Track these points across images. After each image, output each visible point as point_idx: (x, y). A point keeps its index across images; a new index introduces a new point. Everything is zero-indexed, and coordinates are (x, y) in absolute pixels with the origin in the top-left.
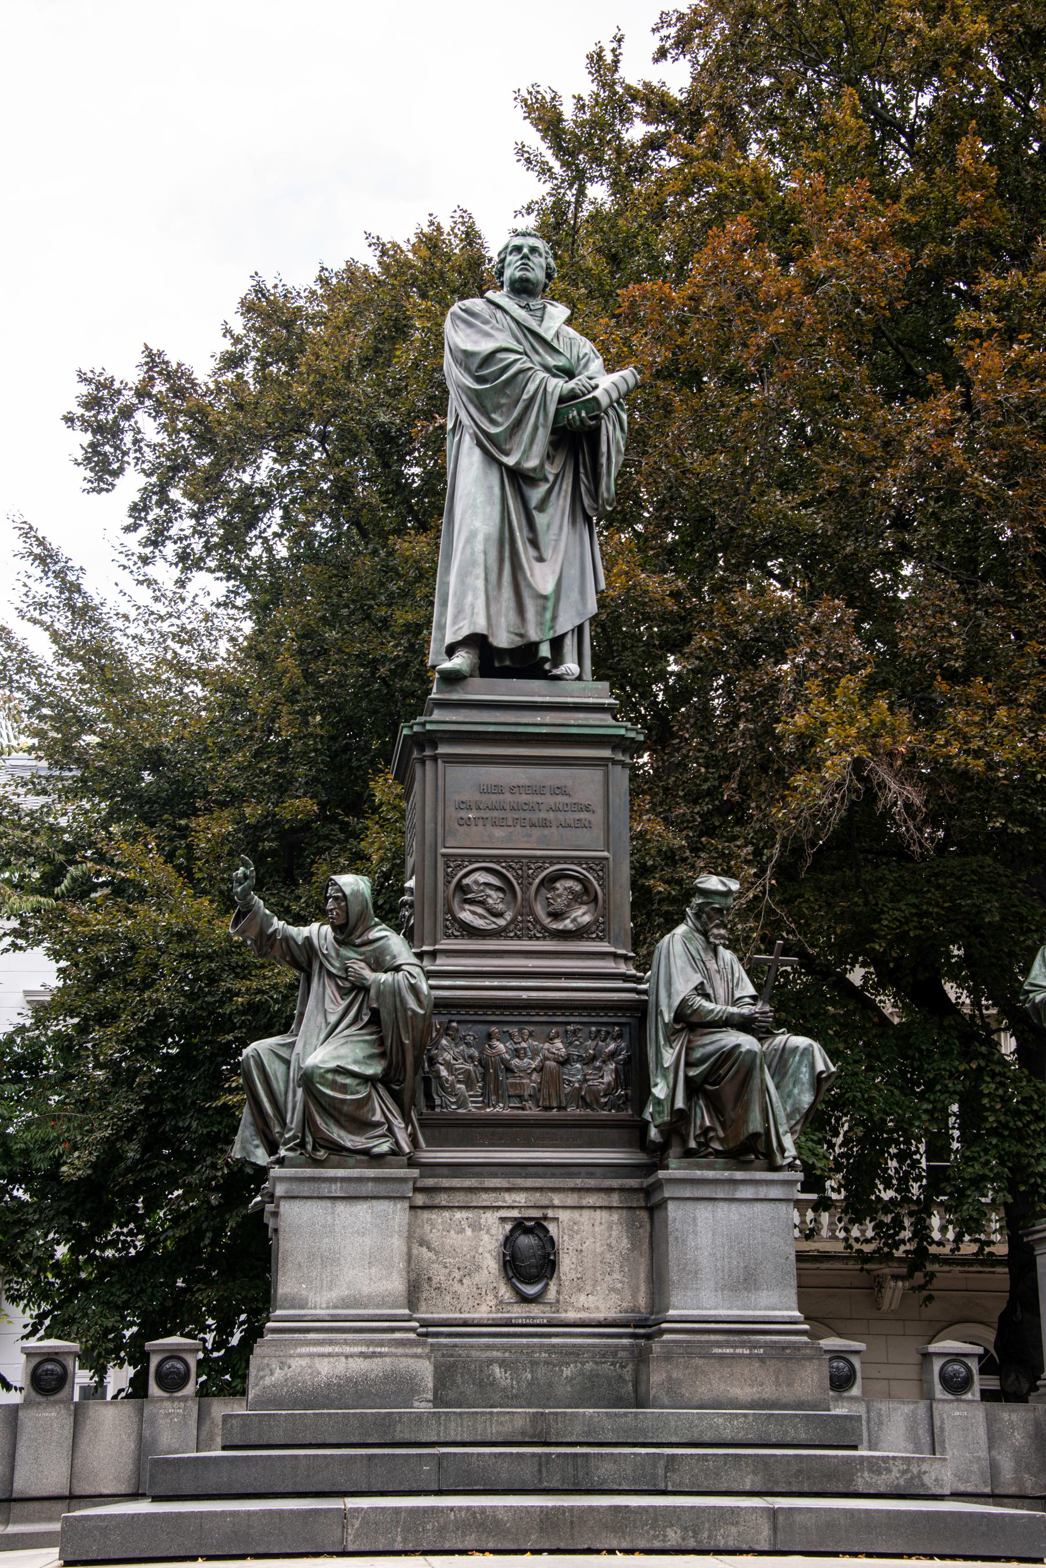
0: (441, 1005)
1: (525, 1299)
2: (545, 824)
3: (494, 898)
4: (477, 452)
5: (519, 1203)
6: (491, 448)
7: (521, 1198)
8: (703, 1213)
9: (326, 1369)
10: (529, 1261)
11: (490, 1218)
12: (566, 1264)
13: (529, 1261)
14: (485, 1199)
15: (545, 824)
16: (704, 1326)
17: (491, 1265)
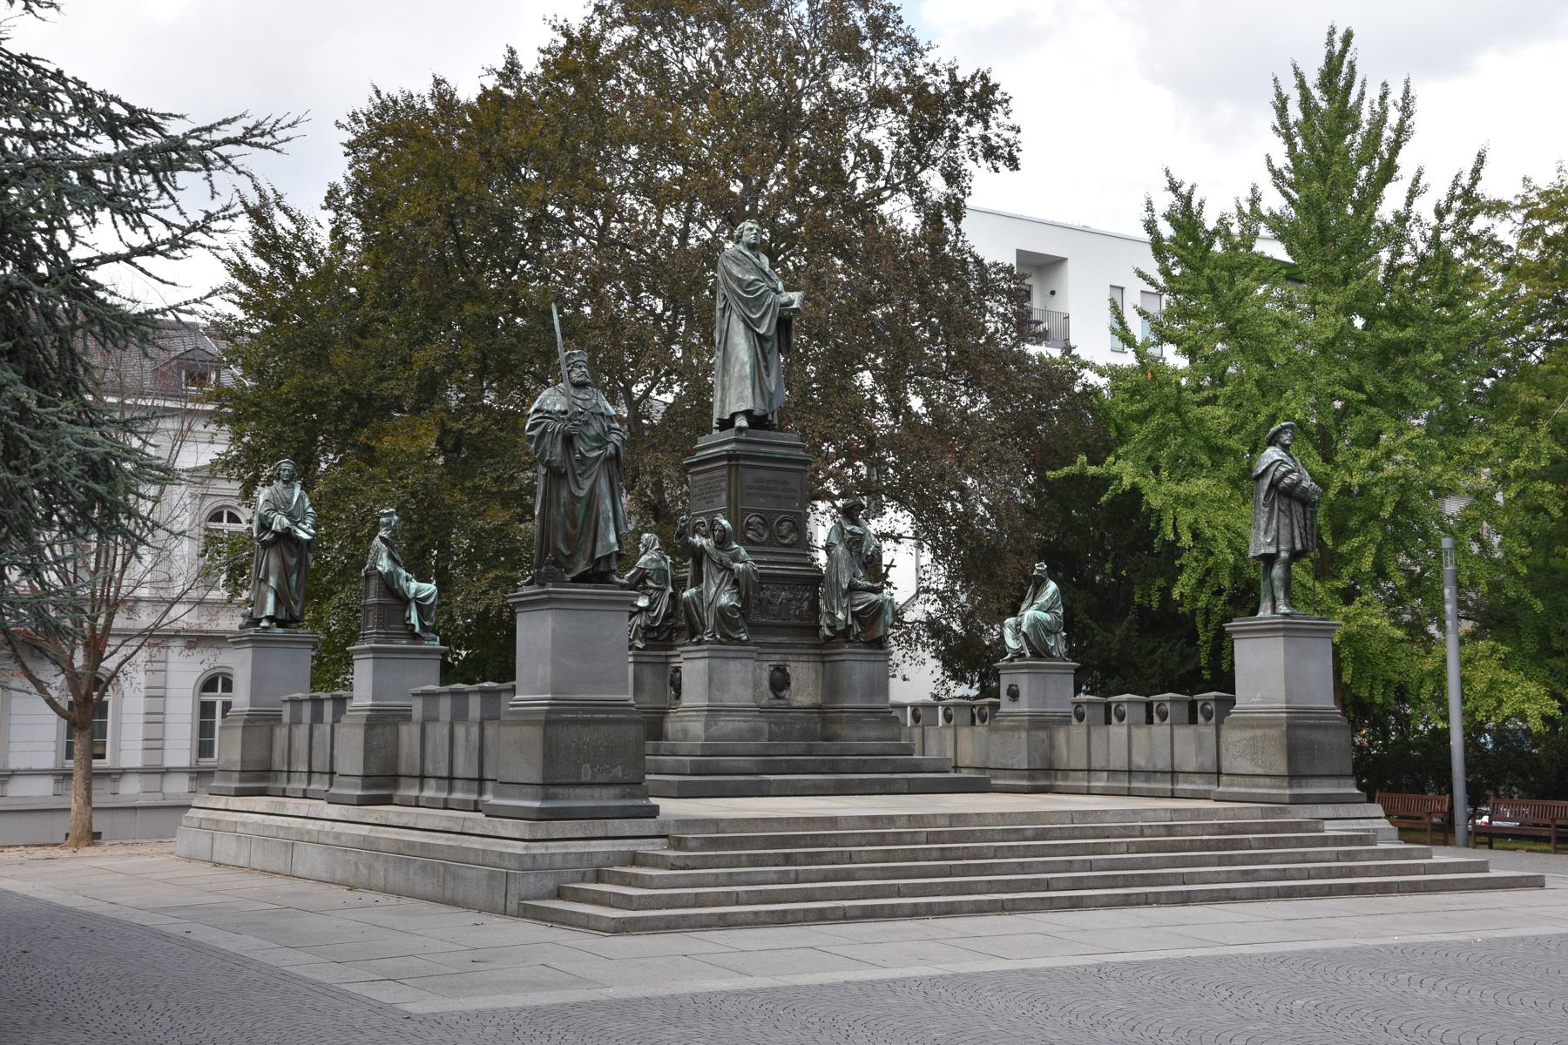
0: (762, 575)
1: (778, 697)
2: (779, 497)
3: (761, 530)
4: (742, 325)
5: (776, 659)
6: (750, 325)
7: (778, 657)
8: (857, 664)
9: (730, 725)
10: (780, 682)
11: (766, 665)
12: (793, 684)
13: (780, 682)
14: (765, 657)
15: (779, 497)
16: (858, 711)
17: (766, 683)
